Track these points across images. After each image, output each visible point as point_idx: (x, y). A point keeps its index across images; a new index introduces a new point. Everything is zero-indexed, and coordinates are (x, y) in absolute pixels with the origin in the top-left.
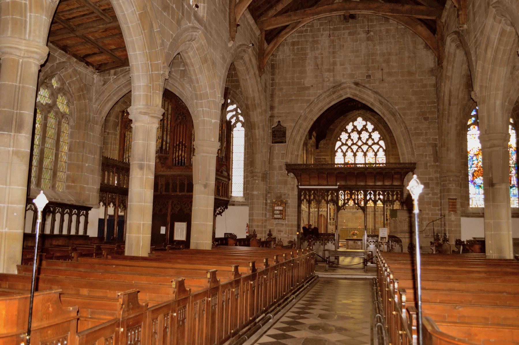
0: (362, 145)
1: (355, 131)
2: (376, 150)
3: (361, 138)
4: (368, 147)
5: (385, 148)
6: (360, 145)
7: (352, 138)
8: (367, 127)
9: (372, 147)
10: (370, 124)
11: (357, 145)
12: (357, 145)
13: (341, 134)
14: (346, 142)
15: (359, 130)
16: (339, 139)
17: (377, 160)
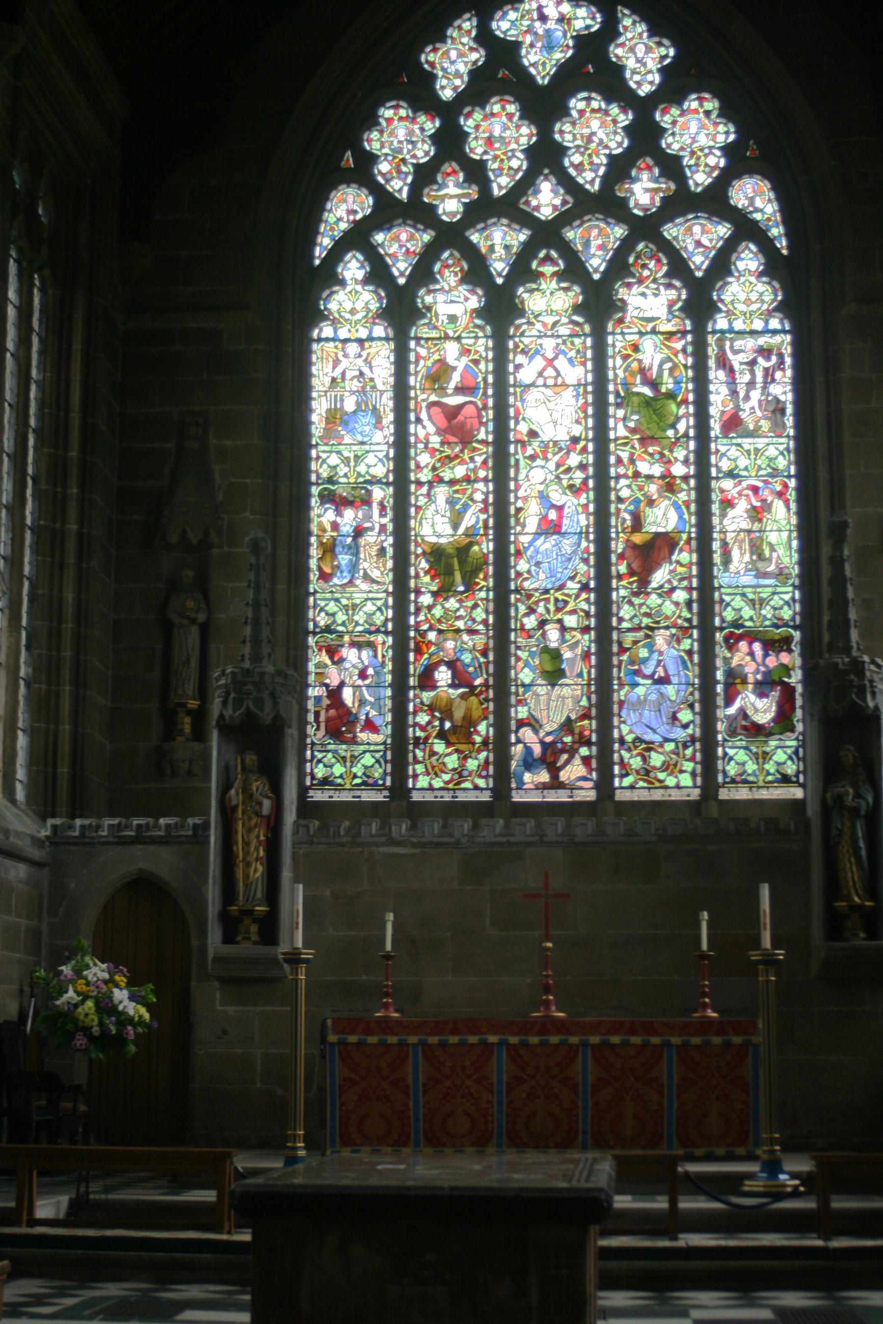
0: (564, 219)
1: (502, 89)
2: (699, 262)
3: (561, 150)
4: (619, 231)
5: (782, 244)
6: (546, 213)
7: (476, 149)
8: (617, 52)
9: (670, 231)
10: (641, 28)
11: (525, 219)
12: (525, 219)
13: (372, 121)
14: (416, 189)
15: (542, 80)
16: (349, 159)
17: (712, 351)
